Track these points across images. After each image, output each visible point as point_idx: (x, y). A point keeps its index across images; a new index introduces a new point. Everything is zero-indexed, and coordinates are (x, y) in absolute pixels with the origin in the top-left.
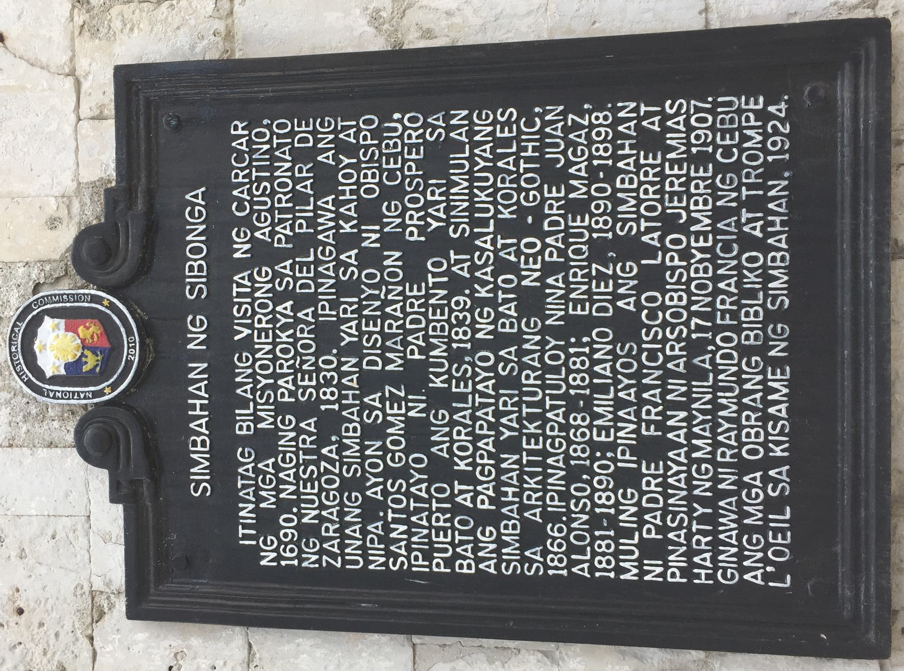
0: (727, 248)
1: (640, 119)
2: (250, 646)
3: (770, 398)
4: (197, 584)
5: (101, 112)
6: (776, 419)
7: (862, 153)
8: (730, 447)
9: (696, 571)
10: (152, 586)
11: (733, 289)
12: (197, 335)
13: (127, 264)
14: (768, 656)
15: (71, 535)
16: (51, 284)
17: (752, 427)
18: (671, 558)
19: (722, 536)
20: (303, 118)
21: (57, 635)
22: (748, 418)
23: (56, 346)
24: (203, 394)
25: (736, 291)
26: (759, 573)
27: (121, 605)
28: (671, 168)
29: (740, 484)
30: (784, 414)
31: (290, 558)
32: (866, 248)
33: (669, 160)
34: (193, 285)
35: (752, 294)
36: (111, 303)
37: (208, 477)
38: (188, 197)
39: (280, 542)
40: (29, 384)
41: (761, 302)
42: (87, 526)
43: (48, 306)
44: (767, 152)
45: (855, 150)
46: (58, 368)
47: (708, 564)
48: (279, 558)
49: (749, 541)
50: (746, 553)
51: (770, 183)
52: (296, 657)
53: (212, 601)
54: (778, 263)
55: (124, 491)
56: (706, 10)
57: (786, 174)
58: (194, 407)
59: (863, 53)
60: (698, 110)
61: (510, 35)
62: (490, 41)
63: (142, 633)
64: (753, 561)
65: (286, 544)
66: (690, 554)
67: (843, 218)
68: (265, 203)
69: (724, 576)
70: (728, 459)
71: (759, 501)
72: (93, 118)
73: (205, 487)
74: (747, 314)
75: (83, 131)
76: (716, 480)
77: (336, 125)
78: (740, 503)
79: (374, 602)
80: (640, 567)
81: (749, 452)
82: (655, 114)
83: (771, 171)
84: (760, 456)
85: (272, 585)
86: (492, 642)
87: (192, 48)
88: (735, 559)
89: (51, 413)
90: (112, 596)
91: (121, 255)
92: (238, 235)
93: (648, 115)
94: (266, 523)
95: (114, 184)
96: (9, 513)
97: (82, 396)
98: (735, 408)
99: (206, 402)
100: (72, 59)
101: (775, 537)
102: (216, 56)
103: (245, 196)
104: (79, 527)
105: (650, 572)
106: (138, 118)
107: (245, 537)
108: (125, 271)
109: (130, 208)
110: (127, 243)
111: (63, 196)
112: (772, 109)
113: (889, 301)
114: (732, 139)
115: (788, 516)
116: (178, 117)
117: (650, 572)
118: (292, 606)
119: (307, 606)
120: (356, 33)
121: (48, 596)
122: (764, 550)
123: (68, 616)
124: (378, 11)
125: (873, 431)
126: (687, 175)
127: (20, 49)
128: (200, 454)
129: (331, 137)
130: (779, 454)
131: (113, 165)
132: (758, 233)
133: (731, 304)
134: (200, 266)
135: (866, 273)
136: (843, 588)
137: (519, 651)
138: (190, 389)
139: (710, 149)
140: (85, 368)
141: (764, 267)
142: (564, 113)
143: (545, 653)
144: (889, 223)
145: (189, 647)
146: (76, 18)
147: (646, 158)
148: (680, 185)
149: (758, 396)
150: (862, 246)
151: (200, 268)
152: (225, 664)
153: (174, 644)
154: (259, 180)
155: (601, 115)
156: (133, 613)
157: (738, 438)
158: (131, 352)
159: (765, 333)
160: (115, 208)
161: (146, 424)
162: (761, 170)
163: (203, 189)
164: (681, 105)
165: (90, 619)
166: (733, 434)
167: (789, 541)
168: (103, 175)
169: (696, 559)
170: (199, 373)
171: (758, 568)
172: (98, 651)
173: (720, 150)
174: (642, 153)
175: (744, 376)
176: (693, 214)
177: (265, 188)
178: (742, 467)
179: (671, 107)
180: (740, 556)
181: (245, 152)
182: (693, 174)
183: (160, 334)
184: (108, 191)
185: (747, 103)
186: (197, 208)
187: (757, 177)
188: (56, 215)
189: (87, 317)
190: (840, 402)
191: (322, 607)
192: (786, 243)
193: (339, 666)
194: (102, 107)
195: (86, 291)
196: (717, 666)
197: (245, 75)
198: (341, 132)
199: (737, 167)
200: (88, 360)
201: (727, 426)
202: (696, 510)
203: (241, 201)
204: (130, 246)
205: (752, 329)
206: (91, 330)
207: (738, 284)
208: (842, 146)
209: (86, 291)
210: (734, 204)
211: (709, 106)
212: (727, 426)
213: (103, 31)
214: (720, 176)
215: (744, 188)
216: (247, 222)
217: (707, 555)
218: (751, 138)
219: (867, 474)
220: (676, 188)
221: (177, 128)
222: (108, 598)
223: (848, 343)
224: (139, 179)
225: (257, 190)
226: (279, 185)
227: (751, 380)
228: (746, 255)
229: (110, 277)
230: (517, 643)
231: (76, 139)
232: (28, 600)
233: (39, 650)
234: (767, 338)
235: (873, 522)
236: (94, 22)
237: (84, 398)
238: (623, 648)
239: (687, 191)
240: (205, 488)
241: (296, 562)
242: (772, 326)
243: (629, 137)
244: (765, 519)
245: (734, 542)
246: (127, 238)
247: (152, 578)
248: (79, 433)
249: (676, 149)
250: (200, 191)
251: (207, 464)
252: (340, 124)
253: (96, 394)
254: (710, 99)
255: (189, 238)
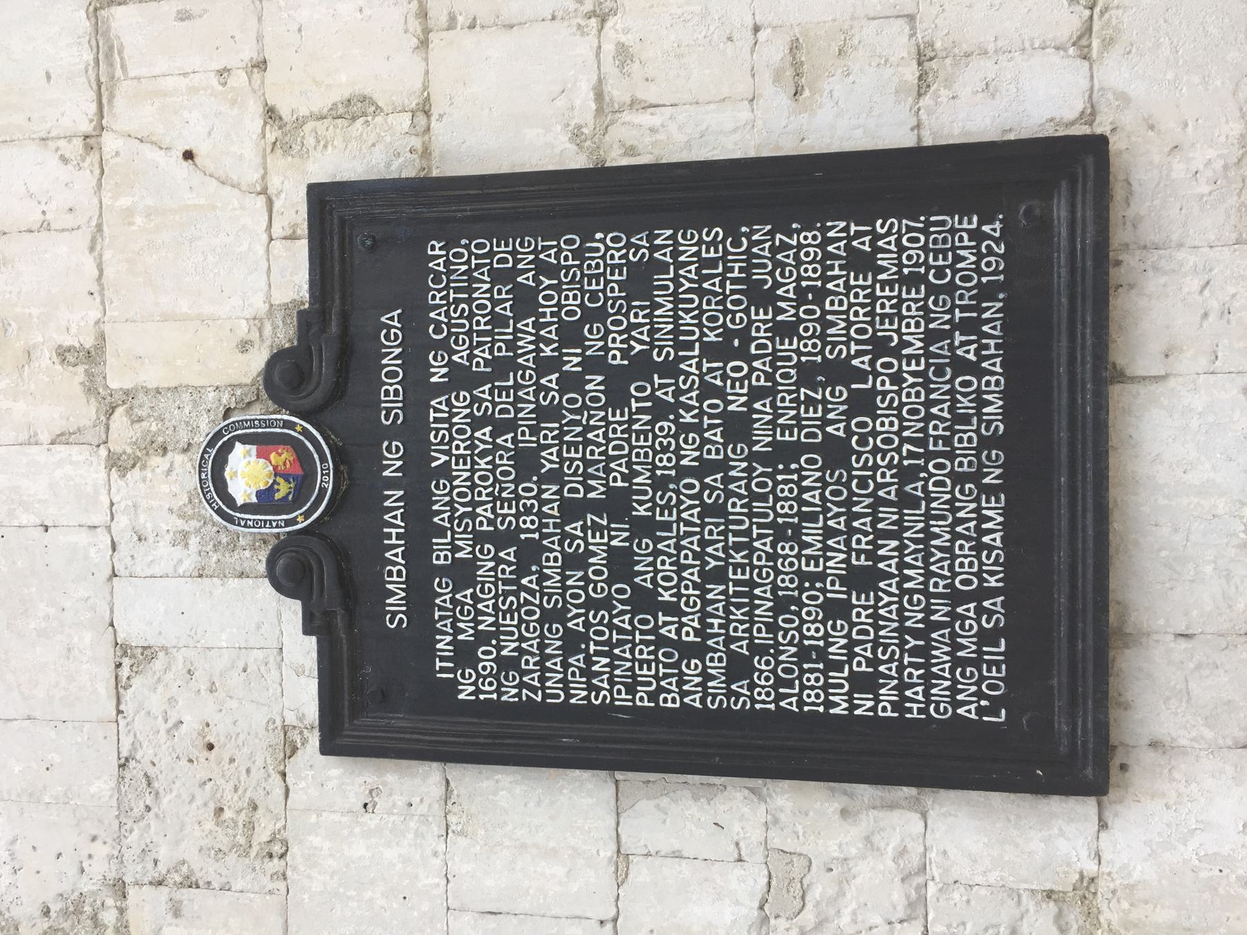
0: (940, 372)
1: (850, 239)
2: (448, 782)
3: (984, 526)
4: (392, 718)
5: (294, 232)
6: (991, 548)
7: (1079, 274)
8: (943, 577)
9: (907, 705)
10: (346, 720)
11: (946, 415)
12: (393, 461)
13: (321, 388)
14: (982, 793)
15: (263, 668)
16: (243, 409)
17: (966, 556)
18: (882, 691)
19: (934, 669)
20: (502, 238)
21: (248, 771)
22: (961, 547)
23: (247, 473)
24: (399, 522)
25: (949, 416)
26: (973, 707)
27: (314, 740)
28: (883, 290)
29: (953, 615)
30: (998, 543)
31: (489, 692)
32: (1083, 373)
33: (880, 281)
34: (389, 410)
35: (966, 419)
36: (304, 428)
37: (404, 608)
38: (383, 319)
39: (479, 675)
40: (219, 512)
41: (974, 428)
42: (279, 658)
43: (239, 432)
44: (981, 273)
45: (1072, 271)
46: (249, 496)
47: (920, 697)
48: (478, 691)
49: (963, 674)
50: (960, 686)
51: (984, 305)
52: (495, 793)
53: (407, 736)
54: (993, 388)
55: (317, 623)
56: (918, 126)
57: (1001, 296)
58: (389, 536)
59: (1080, 170)
60: (910, 229)
61: (715, 152)
62: (695, 159)
63: (336, 769)
64: (965, 694)
65: (485, 677)
66: (902, 687)
67: (1059, 341)
68: (463, 326)
69: (937, 710)
70: (941, 590)
71: (973, 633)
72: (285, 238)
73: (401, 619)
74: (961, 440)
75: (276, 252)
76: (928, 611)
77: (536, 246)
78: (953, 635)
79: (576, 738)
80: (850, 701)
81: (963, 582)
82: (865, 234)
83: (986, 292)
84: (974, 586)
85: (471, 720)
86: (697, 779)
87: (388, 165)
88: (948, 693)
89: (242, 542)
90: (305, 731)
91: (315, 379)
92: (435, 359)
93: (859, 235)
94: (464, 655)
95: (307, 306)
96: (199, 645)
97: (274, 524)
98: (948, 537)
99: (402, 530)
100: (264, 177)
101: (989, 670)
102: (412, 175)
103: (443, 318)
104: (271, 659)
105: (860, 706)
106: (332, 238)
107: (443, 670)
108: (318, 396)
109: (323, 330)
110: (321, 367)
111: (254, 319)
112: (986, 228)
113: (1107, 426)
114: (945, 259)
115: (1003, 649)
116: (374, 237)
117: (860, 706)
118: (490, 741)
119: (507, 741)
120: (557, 151)
121: (239, 730)
122: (978, 684)
123: (261, 754)
124: (579, 127)
125: (1090, 561)
126: (899, 296)
127: (211, 167)
128: (396, 585)
129: (531, 257)
130: (994, 584)
131: (306, 287)
132: (971, 357)
133: (944, 429)
134: (396, 391)
135: (1083, 398)
136: (1060, 723)
137: (725, 787)
138: (386, 517)
139: (922, 270)
140: (278, 496)
141: (978, 391)
142: (771, 233)
143: (752, 790)
144: (1107, 346)
145: (385, 784)
146: (268, 135)
147: (856, 279)
148: (892, 307)
149: (972, 524)
150: (1079, 370)
151: (396, 392)
152: (422, 801)
153: (369, 780)
154: (457, 301)
155: (810, 235)
156: (328, 748)
157: (951, 567)
158: (325, 480)
159: (979, 459)
160: (308, 331)
161: (340, 553)
162: (974, 292)
163: (399, 311)
164: (892, 225)
165: (282, 755)
166: (946, 563)
167: (1004, 674)
168: (296, 297)
169: (908, 693)
170: (395, 501)
171: (972, 702)
172: (291, 787)
173: (933, 271)
174: (852, 274)
175: (957, 504)
176: (904, 337)
177: (463, 310)
178: (956, 597)
179: (882, 226)
180: (954, 690)
181: (442, 273)
182: (904, 296)
183: (354, 460)
184: (301, 314)
185: (960, 223)
186: (393, 331)
187: (970, 298)
188: (247, 338)
189: (280, 444)
190: (1056, 531)
191: (522, 742)
192: (1001, 367)
193: (539, 803)
194: (294, 226)
195: (279, 417)
196: (930, 803)
197: (442, 193)
198: (542, 252)
199: (951, 288)
200: (281, 487)
201: (939, 555)
202: (907, 642)
203: (438, 324)
204: (324, 370)
205: (965, 456)
206: (284, 456)
207: (952, 409)
208: (1059, 267)
209: (279, 417)
210: (947, 327)
211: (921, 225)
212: (939, 555)
213: (296, 148)
214: (932, 298)
215: (957, 310)
216: (444, 345)
217: (920, 689)
218: (964, 259)
219: (1084, 605)
220: (887, 310)
221: (373, 248)
222: (301, 733)
223: (1064, 470)
224: (333, 301)
225: (455, 312)
226: (478, 307)
227: (964, 508)
228: (960, 379)
229: (301, 402)
230: (723, 779)
231: (268, 260)
232: (218, 735)
233: (230, 786)
234: (981, 465)
235: (1090, 655)
236: (287, 139)
237: (276, 527)
238: (832, 784)
239: (899, 314)
240: (401, 620)
241: (495, 696)
242: (986, 452)
243: (838, 257)
244: (979, 652)
245: (947, 675)
246: (321, 362)
247: (346, 712)
248: (271, 563)
249: (887, 269)
250: (395, 313)
251: (403, 594)
252: (540, 244)
253: (288, 523)
254: (922, 218)
255: (384, 362)
